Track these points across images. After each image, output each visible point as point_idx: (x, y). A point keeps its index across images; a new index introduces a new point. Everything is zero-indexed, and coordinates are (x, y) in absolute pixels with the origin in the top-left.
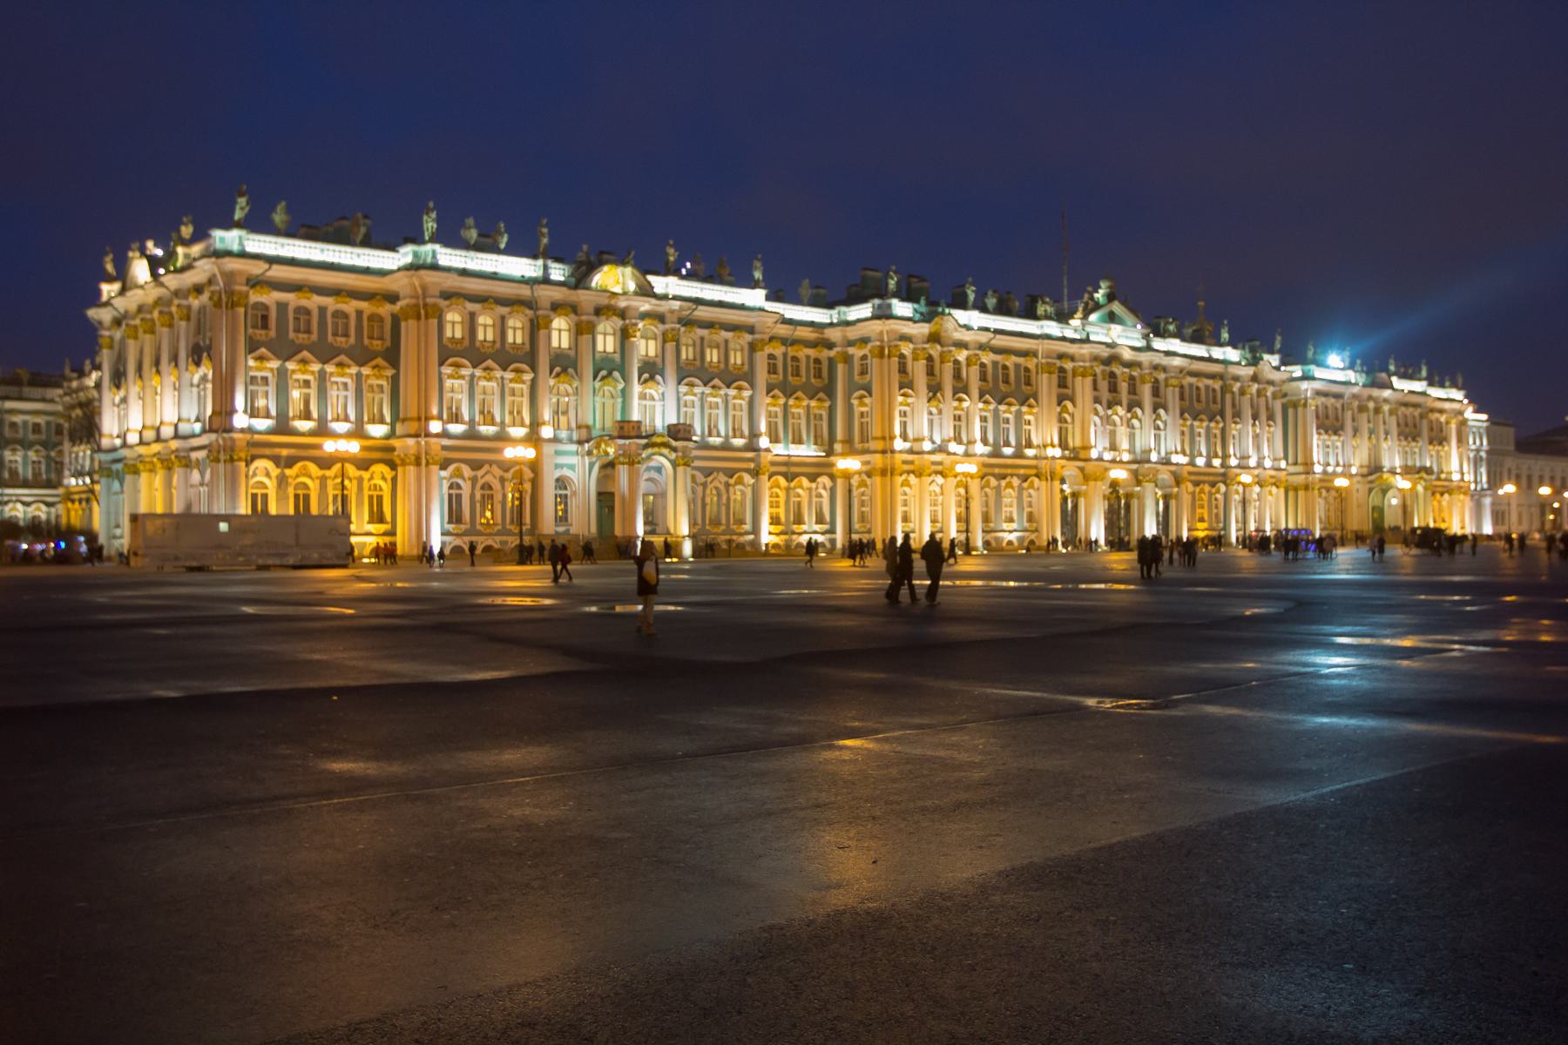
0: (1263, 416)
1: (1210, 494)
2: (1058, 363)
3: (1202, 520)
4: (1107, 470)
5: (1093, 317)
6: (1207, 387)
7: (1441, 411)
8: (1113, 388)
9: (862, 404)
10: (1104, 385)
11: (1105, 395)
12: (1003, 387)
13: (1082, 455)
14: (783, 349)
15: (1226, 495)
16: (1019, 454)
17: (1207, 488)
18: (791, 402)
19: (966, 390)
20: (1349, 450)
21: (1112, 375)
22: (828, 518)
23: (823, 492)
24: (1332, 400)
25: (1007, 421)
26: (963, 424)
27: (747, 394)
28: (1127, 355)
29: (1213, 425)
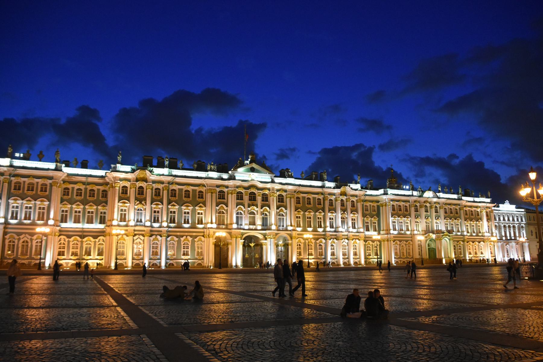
2: (218, 189)
4: (214, 233)
7: (477, 207)
12: (185, 199)
13: (229, 227)
14: (84, 186)
15: (326, 244)
16: (193, 227)
18: (87, 207)
20: (413, 223)
27: (47, 203)
28: (260, 185)
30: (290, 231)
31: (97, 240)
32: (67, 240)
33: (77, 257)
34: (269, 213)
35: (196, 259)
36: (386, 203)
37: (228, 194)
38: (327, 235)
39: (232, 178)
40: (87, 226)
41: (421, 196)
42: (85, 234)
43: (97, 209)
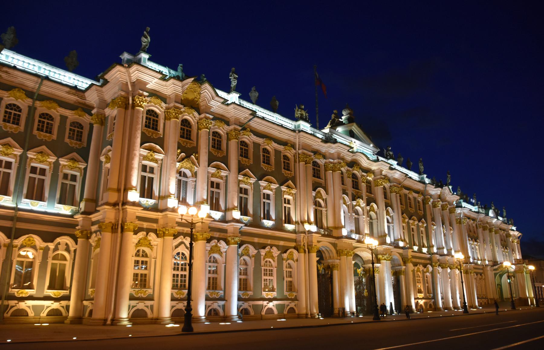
0: (447, 223)
1: (424, 273)
3: (420, 292)
5: (340, 129)
6: (415, 198)
8: (356, 185)
10: (349, 181)
11: (350, 190)
12: (264, 166)
13: (335, 233)
14: (29, 101)
16: (278, 227)
17: (421, 268)
18: (31, 155)
19: (225, 160)
21: (354, 176)
24: (472, 222)
25: (268, 197)
26: (222, 192)
28: (365, 163)
29: (420, 224)
30: (402, 248)
31: (51, 246)
34: (376, 213)
35: (287, 299)
36: (460, 219)
37: (326, 170)
38: (433, 259)
39: (328, 140)
40: (26, 204)
41: (487, 214)
42: (21, 226)
43: (56, 165)
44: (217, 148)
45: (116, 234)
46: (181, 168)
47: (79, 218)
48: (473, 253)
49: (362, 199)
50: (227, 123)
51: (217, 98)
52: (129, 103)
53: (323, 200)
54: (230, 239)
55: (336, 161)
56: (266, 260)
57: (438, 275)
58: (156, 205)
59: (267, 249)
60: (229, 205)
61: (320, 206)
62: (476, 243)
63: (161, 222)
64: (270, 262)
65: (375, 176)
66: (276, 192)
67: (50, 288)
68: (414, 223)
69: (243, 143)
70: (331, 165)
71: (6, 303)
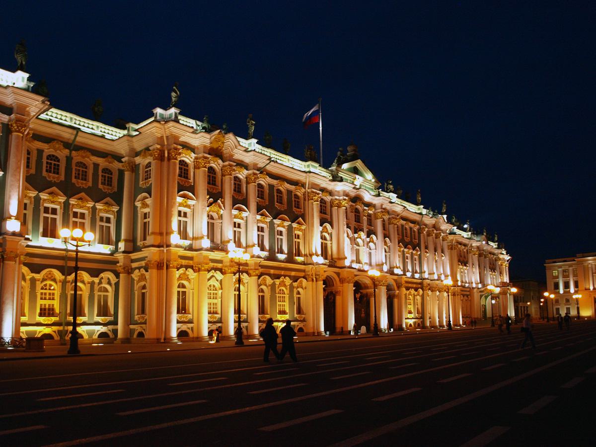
0: (439, 250)
1: (415, 296)
6: (411, 228)
8: (358, 219)
9: (145, 205)
10: (352, 216)
11: (353, 224)
12: (277, 205)
13: (339, 264)
16: (290, 260)
17: (413, 291)
19: (245, 202)
22: (112, 311)
23: (108, 287)
24: (463, 247)
25: (281, 233)
26: (242, 230)
31: (96, 280)
32: (29, 275)
33: (54, 319)
34: (375, 244)
37: (331, 207)
44: (238, 192)
45: (161, 271)
46: (210, 211)
47: (120, 256)
48: (462, 277)
49: (363, 232)
50: (246, 167)
51: (239, 147)
52: (164, 156)
53: (329, 234)
54: (251, 272)
55: (341, 198)
56: (279, 289)
57: (428, 298)
58: (191, 245)
59: (281, 279)
60: (250, 243)
61: (325, 239)
62: (465, 267)
63: (196, 260)
64: (283, 290)
65: (375, 210)
66: (288, 229)
67: (98, 316)
68: (408, 252)
69: (260, 186)
70: (337, 202)
71: (66, 328)
